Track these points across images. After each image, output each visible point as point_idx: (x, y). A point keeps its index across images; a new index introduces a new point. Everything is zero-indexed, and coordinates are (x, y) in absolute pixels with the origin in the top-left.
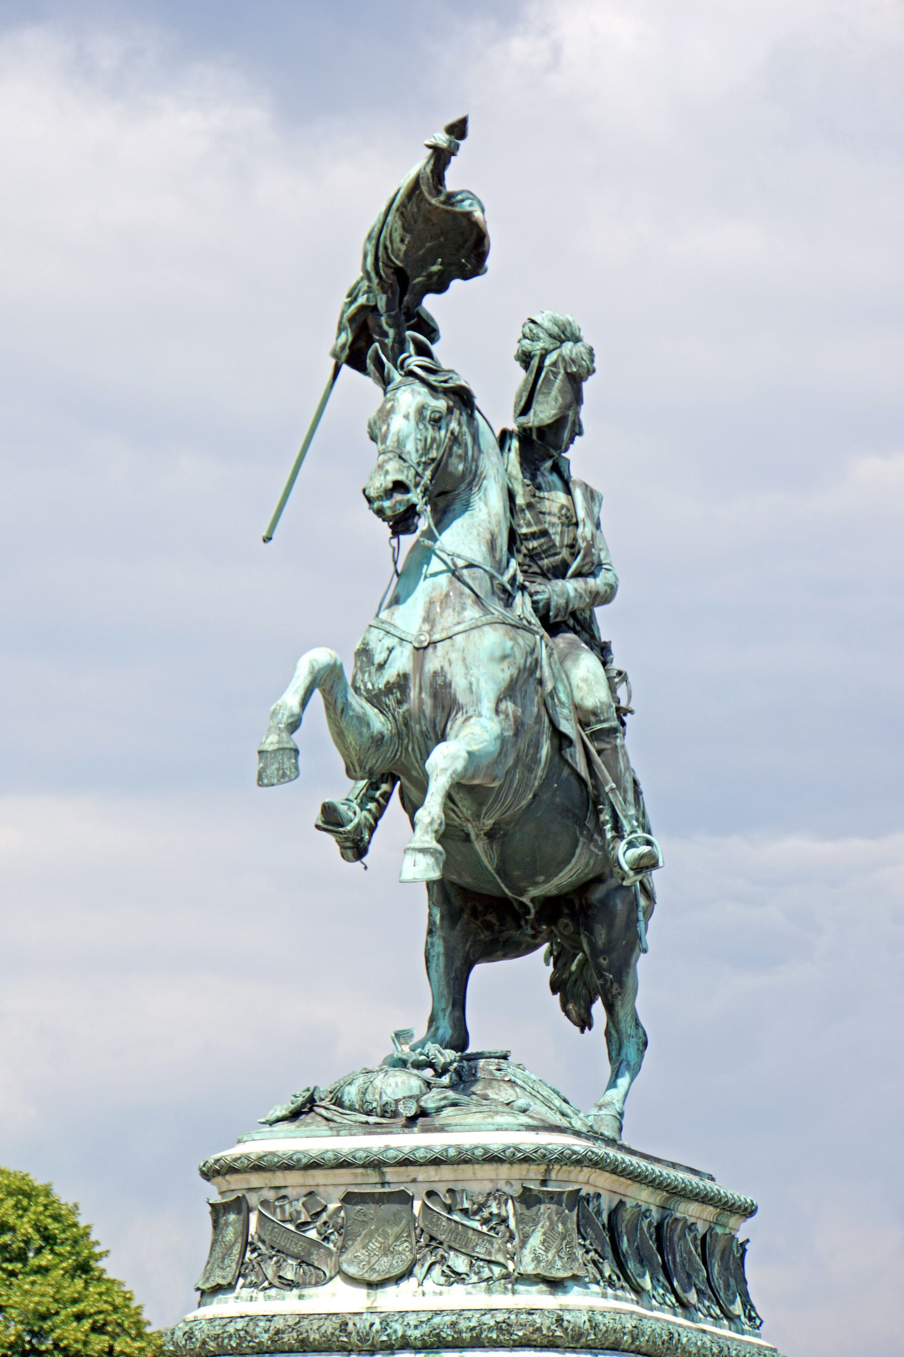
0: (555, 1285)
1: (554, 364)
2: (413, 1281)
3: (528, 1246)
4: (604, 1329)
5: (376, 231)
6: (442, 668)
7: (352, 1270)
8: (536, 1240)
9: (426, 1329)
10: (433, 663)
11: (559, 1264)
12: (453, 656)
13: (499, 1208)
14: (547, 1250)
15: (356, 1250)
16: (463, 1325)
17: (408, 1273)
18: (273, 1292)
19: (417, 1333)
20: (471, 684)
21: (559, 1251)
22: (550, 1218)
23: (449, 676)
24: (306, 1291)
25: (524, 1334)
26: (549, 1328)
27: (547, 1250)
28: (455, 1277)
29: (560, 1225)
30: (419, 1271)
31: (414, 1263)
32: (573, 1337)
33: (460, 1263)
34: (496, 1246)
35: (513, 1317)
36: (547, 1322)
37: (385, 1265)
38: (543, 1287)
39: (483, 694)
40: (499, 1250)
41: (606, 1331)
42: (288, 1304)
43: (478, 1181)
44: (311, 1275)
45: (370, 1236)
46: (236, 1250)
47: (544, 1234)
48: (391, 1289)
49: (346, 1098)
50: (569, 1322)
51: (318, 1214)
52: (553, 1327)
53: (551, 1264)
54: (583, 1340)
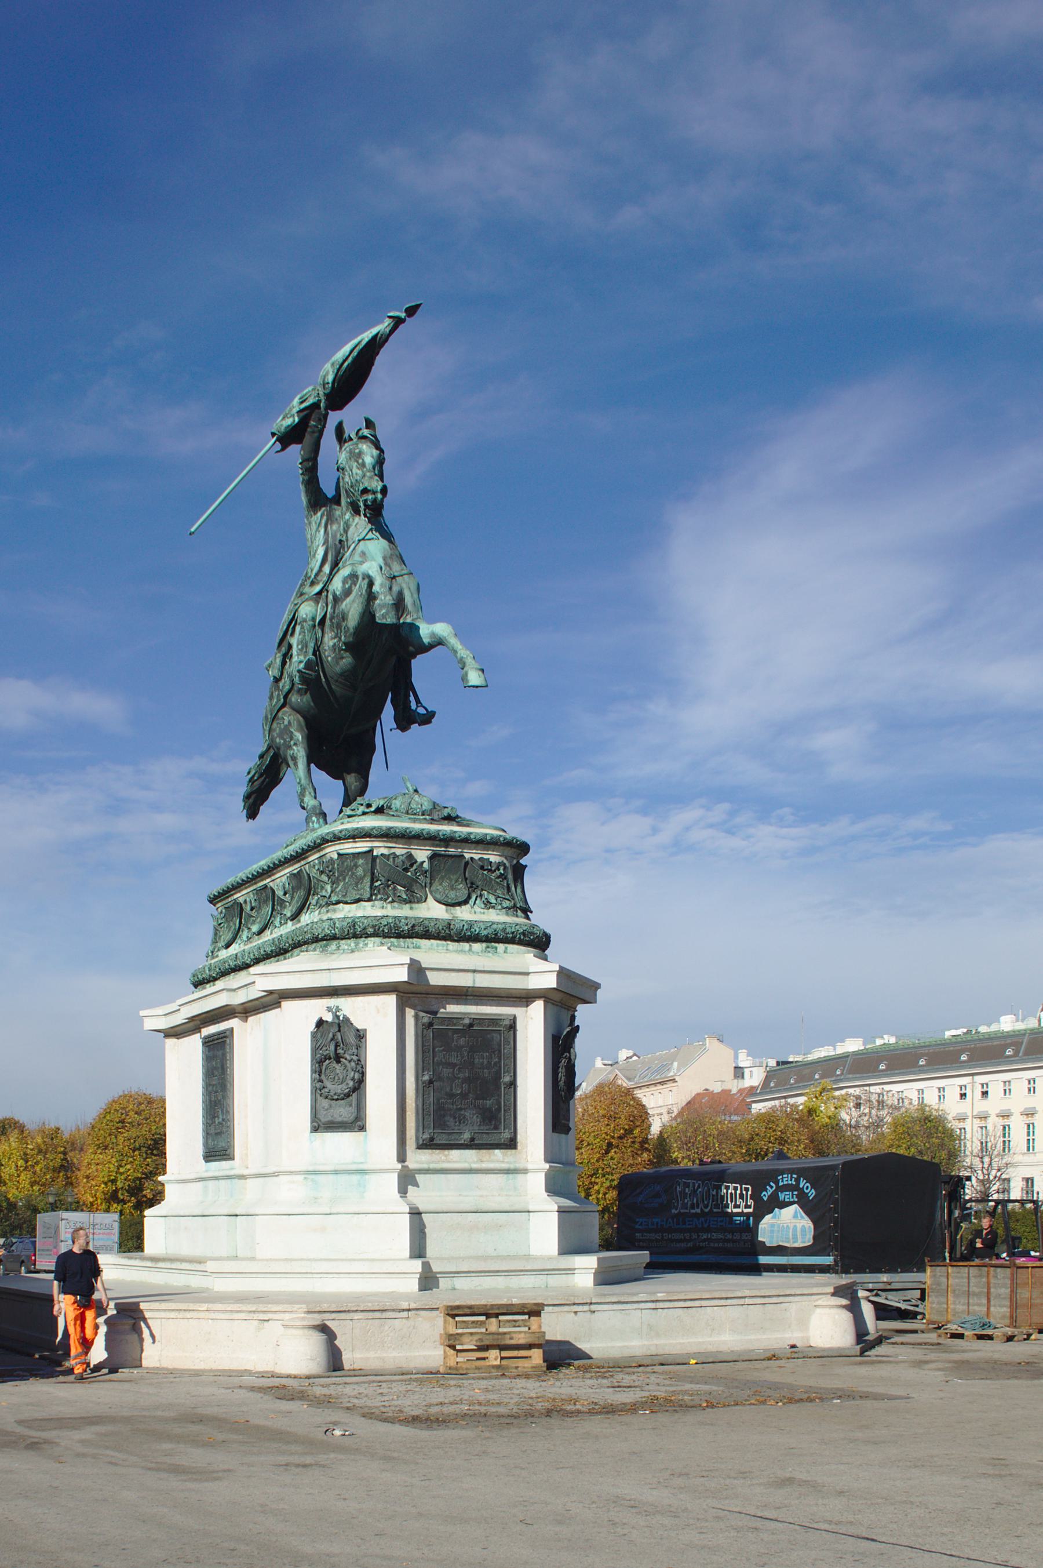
2: (468, 906)
5: (341, 361)
7: (438, 896)
9: (490, 931)
12: (404, 586)
15: (436, 885)
16: (509, 930)
17: (466, 902)
18: (395, 904)
19: (485, 933)
24: (414, 905)
28: (488, 905)
30: (472, 901)
31: (469, 897)
33: (492, 900)
37: (452, 895)
42: (404, 911)
43: (494, 858)
44: (412, 900)
45: (442, 878)
46: (367, 880)
48: (458, 908)
49: (393, 806)
51: (412, 865)
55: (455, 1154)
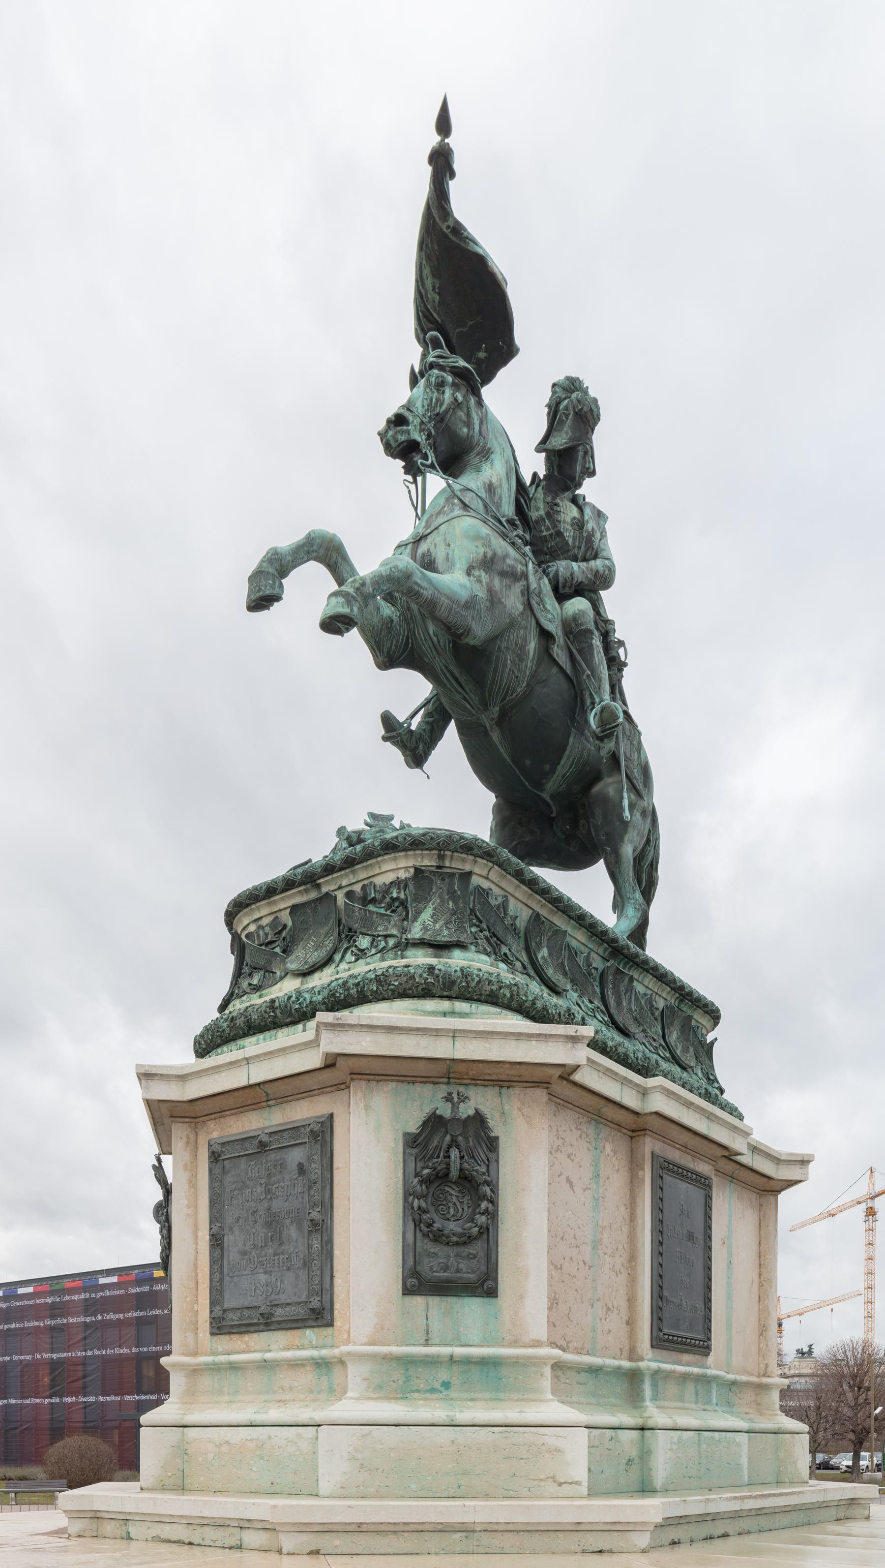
0: (440, 948)
1: (566, 408)
3: (420, 920)
4: (477, 979)
6: (428, 550)
8: (426, 915)
10: (423, 547)
11: (446, 932)
13: (398, 893)
14: (435, 922)
20: (448, 554)
21: (446, 923)
22: (441, 897)
23: (433, 555)
25: (400, 984)
26: (421, 976)
27: (435, 922)
29: (451, 903)
32: (444, 984)
34: (393, 923)
35: (390, 970)
36: (420, 971)
38: (430, 951)
39: (457, 559)
40: (395, 925)
41: (479, 982)
47: (434, 909)
50: (440, 970)
52: (425, 975)
53: (439, 932)
54: (456, 988)
55: (256, 1340)
